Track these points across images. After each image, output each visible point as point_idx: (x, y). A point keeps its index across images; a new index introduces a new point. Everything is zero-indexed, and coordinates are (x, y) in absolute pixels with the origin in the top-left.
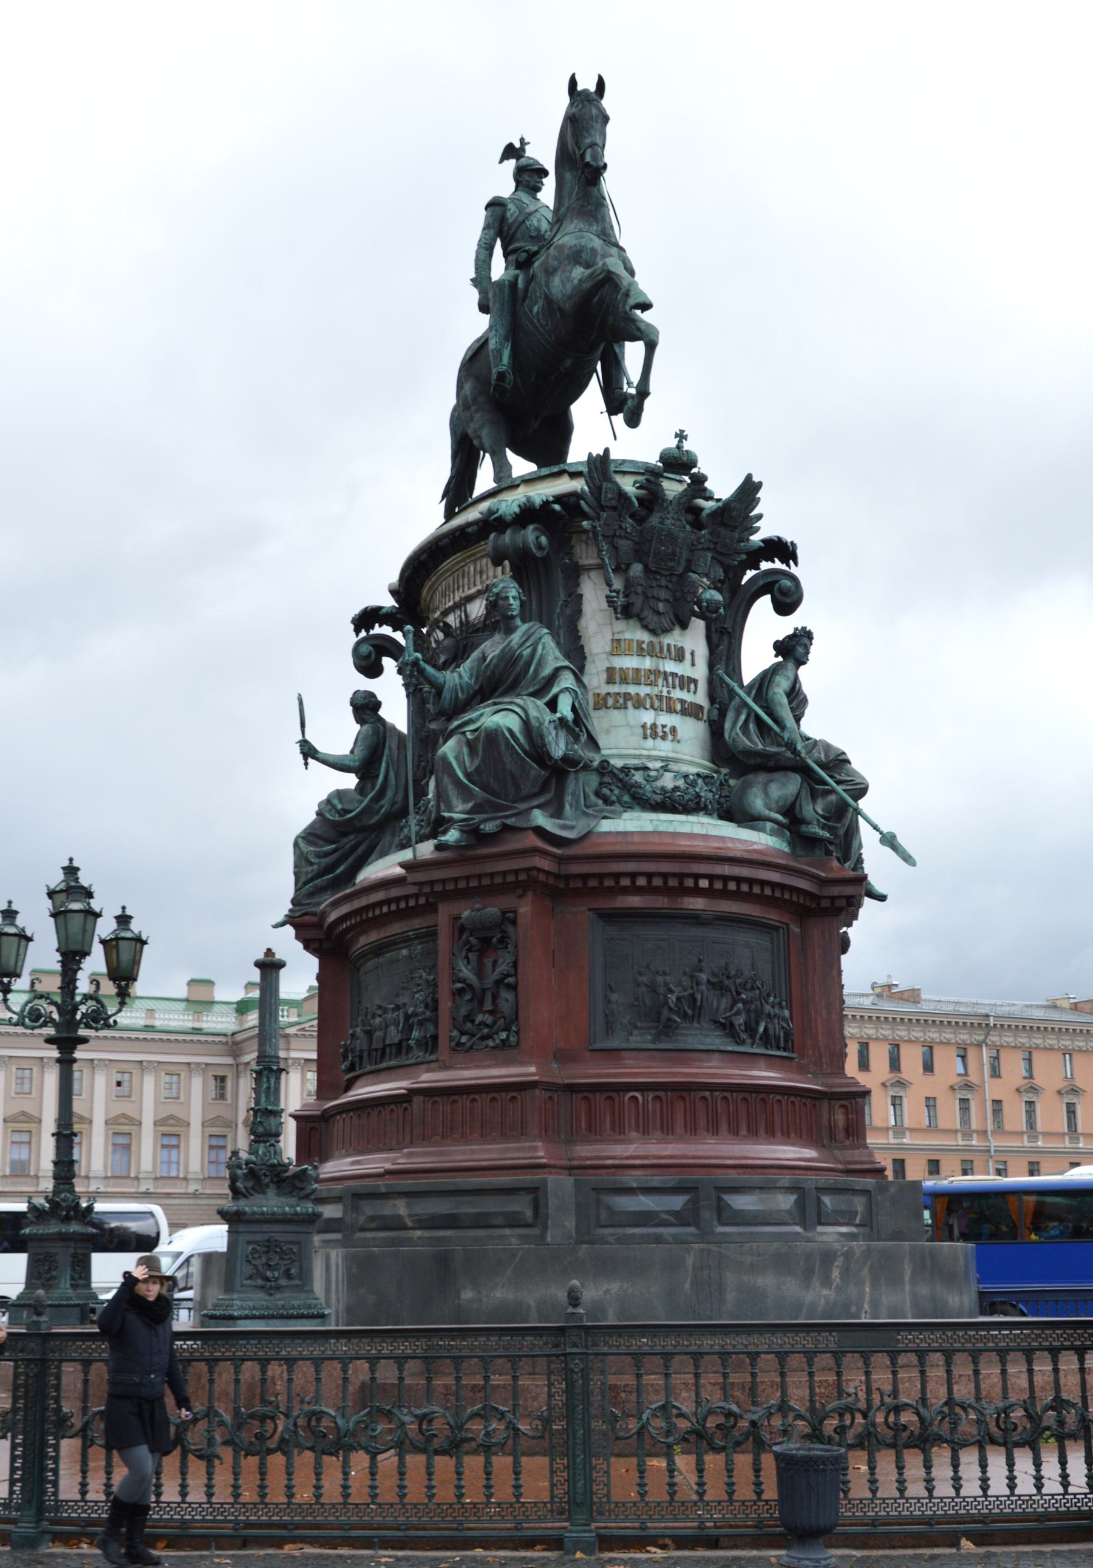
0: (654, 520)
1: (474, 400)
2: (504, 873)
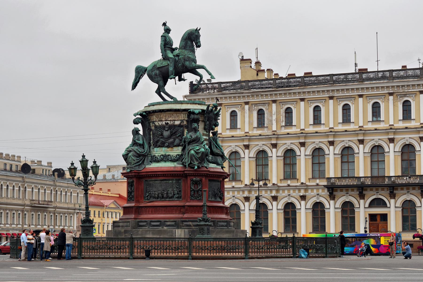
0: (211, 114)
1: (159, 75)
2: (202, 174)
